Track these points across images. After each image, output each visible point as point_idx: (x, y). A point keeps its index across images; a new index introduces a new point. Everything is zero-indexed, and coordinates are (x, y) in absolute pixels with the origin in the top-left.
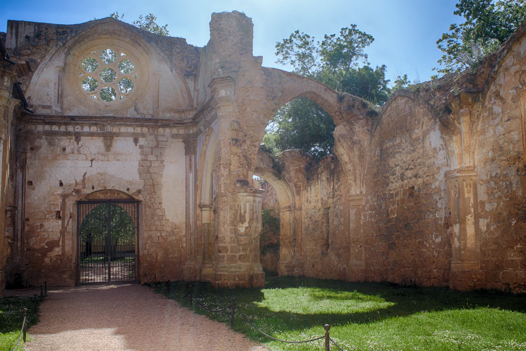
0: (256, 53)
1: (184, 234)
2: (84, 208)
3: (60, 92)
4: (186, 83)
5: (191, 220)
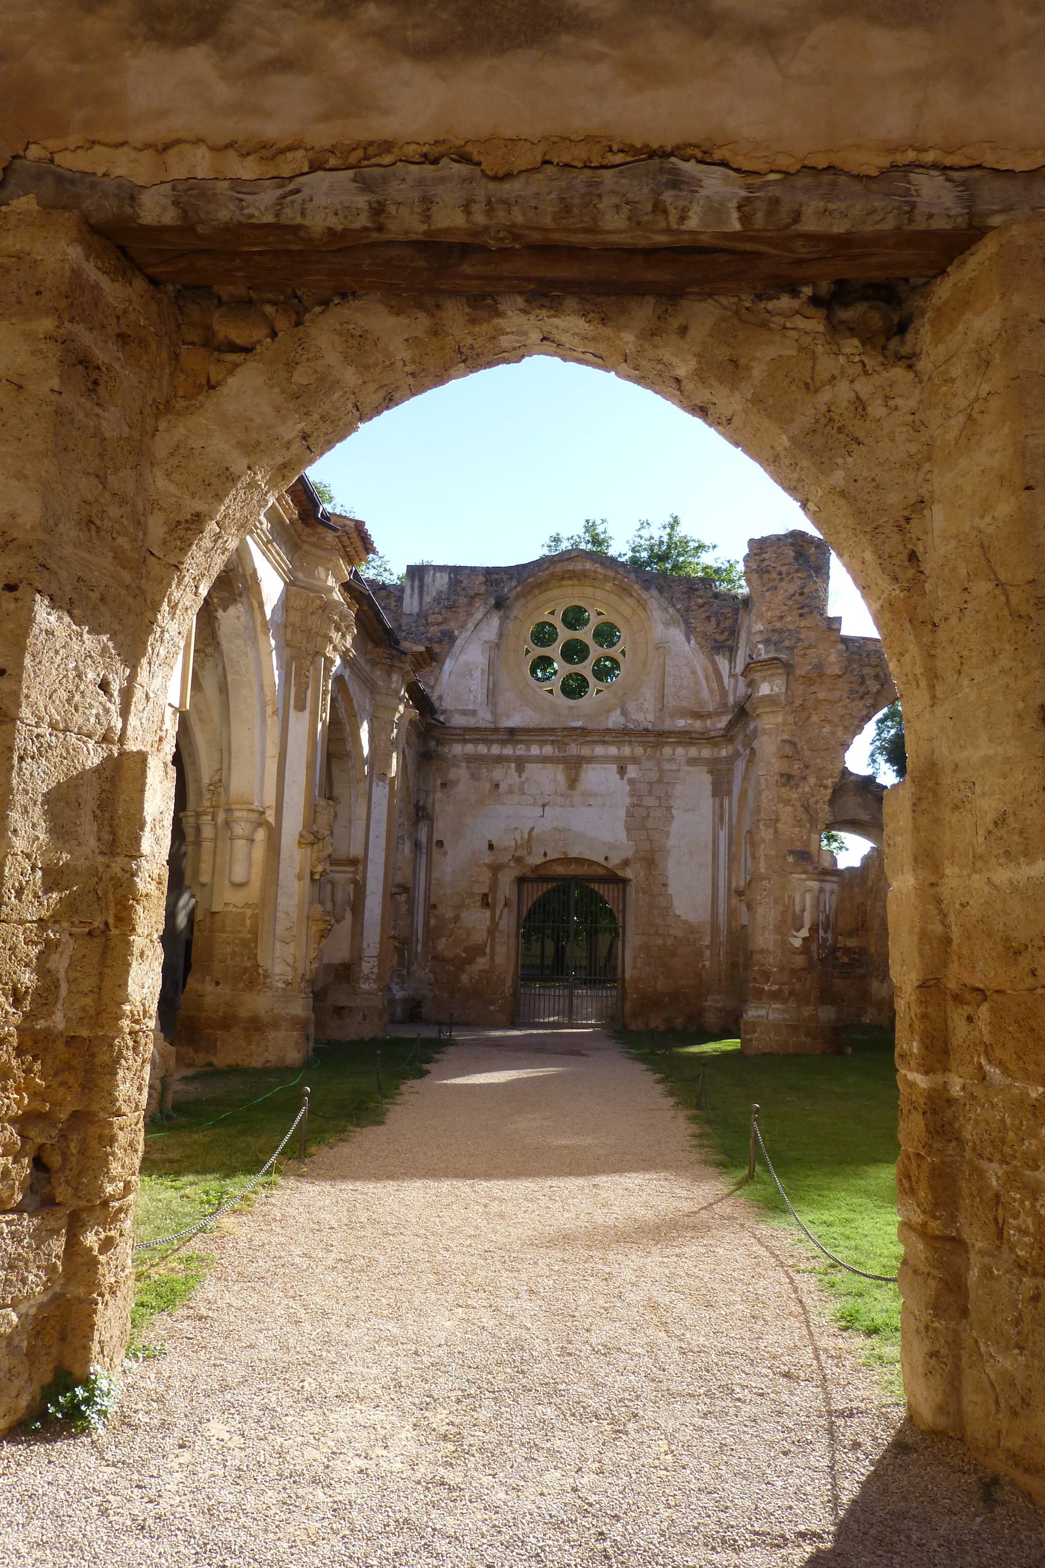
0: (832, 612)
2: (530, 890)
3: (491, 686)
4: (714, 664)
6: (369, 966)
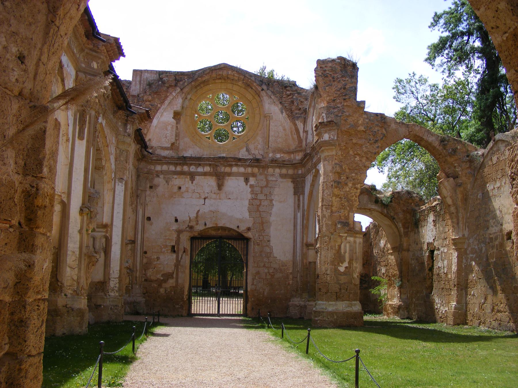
0: (359, 99)
1: (291, 271)
2: (197, 243)
4: (295, 125)
5: (298, 258)
6: (113, 283)
